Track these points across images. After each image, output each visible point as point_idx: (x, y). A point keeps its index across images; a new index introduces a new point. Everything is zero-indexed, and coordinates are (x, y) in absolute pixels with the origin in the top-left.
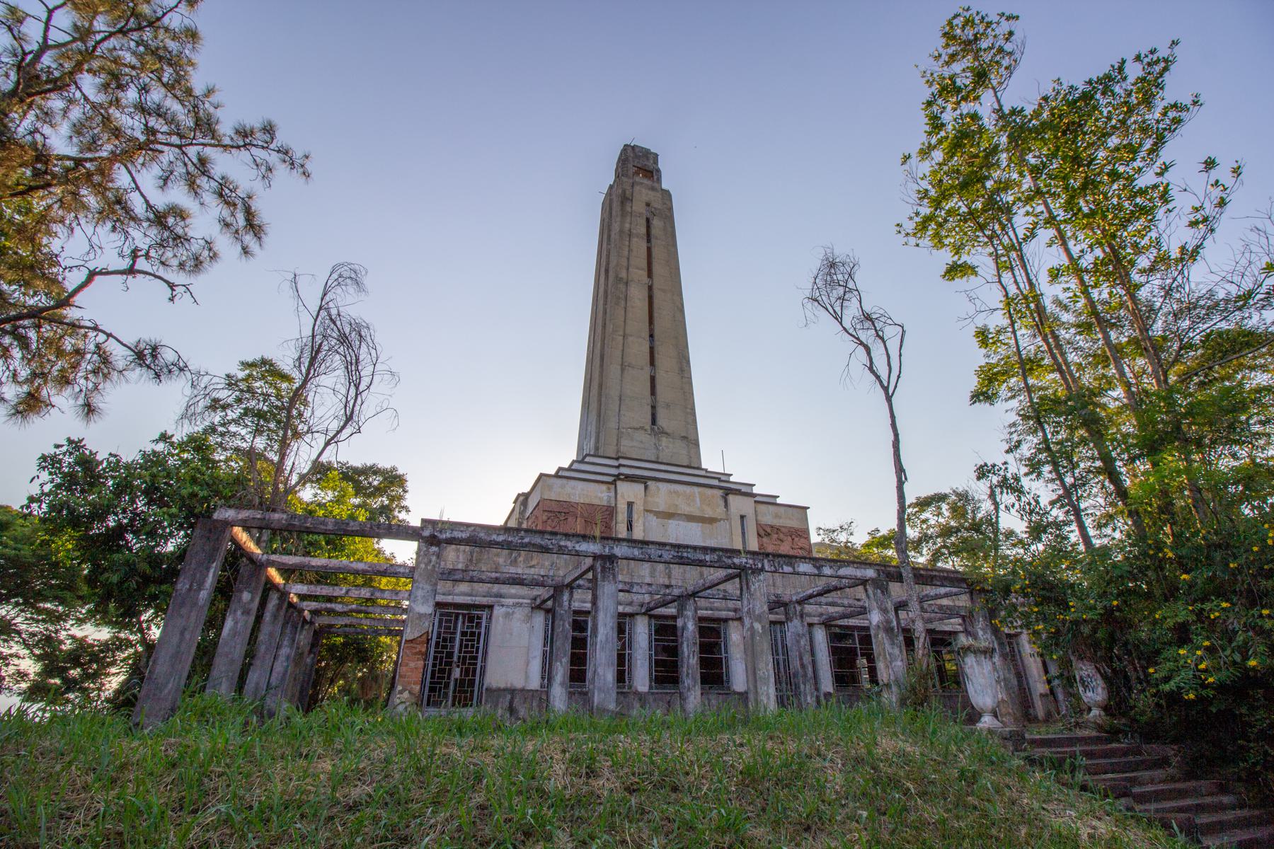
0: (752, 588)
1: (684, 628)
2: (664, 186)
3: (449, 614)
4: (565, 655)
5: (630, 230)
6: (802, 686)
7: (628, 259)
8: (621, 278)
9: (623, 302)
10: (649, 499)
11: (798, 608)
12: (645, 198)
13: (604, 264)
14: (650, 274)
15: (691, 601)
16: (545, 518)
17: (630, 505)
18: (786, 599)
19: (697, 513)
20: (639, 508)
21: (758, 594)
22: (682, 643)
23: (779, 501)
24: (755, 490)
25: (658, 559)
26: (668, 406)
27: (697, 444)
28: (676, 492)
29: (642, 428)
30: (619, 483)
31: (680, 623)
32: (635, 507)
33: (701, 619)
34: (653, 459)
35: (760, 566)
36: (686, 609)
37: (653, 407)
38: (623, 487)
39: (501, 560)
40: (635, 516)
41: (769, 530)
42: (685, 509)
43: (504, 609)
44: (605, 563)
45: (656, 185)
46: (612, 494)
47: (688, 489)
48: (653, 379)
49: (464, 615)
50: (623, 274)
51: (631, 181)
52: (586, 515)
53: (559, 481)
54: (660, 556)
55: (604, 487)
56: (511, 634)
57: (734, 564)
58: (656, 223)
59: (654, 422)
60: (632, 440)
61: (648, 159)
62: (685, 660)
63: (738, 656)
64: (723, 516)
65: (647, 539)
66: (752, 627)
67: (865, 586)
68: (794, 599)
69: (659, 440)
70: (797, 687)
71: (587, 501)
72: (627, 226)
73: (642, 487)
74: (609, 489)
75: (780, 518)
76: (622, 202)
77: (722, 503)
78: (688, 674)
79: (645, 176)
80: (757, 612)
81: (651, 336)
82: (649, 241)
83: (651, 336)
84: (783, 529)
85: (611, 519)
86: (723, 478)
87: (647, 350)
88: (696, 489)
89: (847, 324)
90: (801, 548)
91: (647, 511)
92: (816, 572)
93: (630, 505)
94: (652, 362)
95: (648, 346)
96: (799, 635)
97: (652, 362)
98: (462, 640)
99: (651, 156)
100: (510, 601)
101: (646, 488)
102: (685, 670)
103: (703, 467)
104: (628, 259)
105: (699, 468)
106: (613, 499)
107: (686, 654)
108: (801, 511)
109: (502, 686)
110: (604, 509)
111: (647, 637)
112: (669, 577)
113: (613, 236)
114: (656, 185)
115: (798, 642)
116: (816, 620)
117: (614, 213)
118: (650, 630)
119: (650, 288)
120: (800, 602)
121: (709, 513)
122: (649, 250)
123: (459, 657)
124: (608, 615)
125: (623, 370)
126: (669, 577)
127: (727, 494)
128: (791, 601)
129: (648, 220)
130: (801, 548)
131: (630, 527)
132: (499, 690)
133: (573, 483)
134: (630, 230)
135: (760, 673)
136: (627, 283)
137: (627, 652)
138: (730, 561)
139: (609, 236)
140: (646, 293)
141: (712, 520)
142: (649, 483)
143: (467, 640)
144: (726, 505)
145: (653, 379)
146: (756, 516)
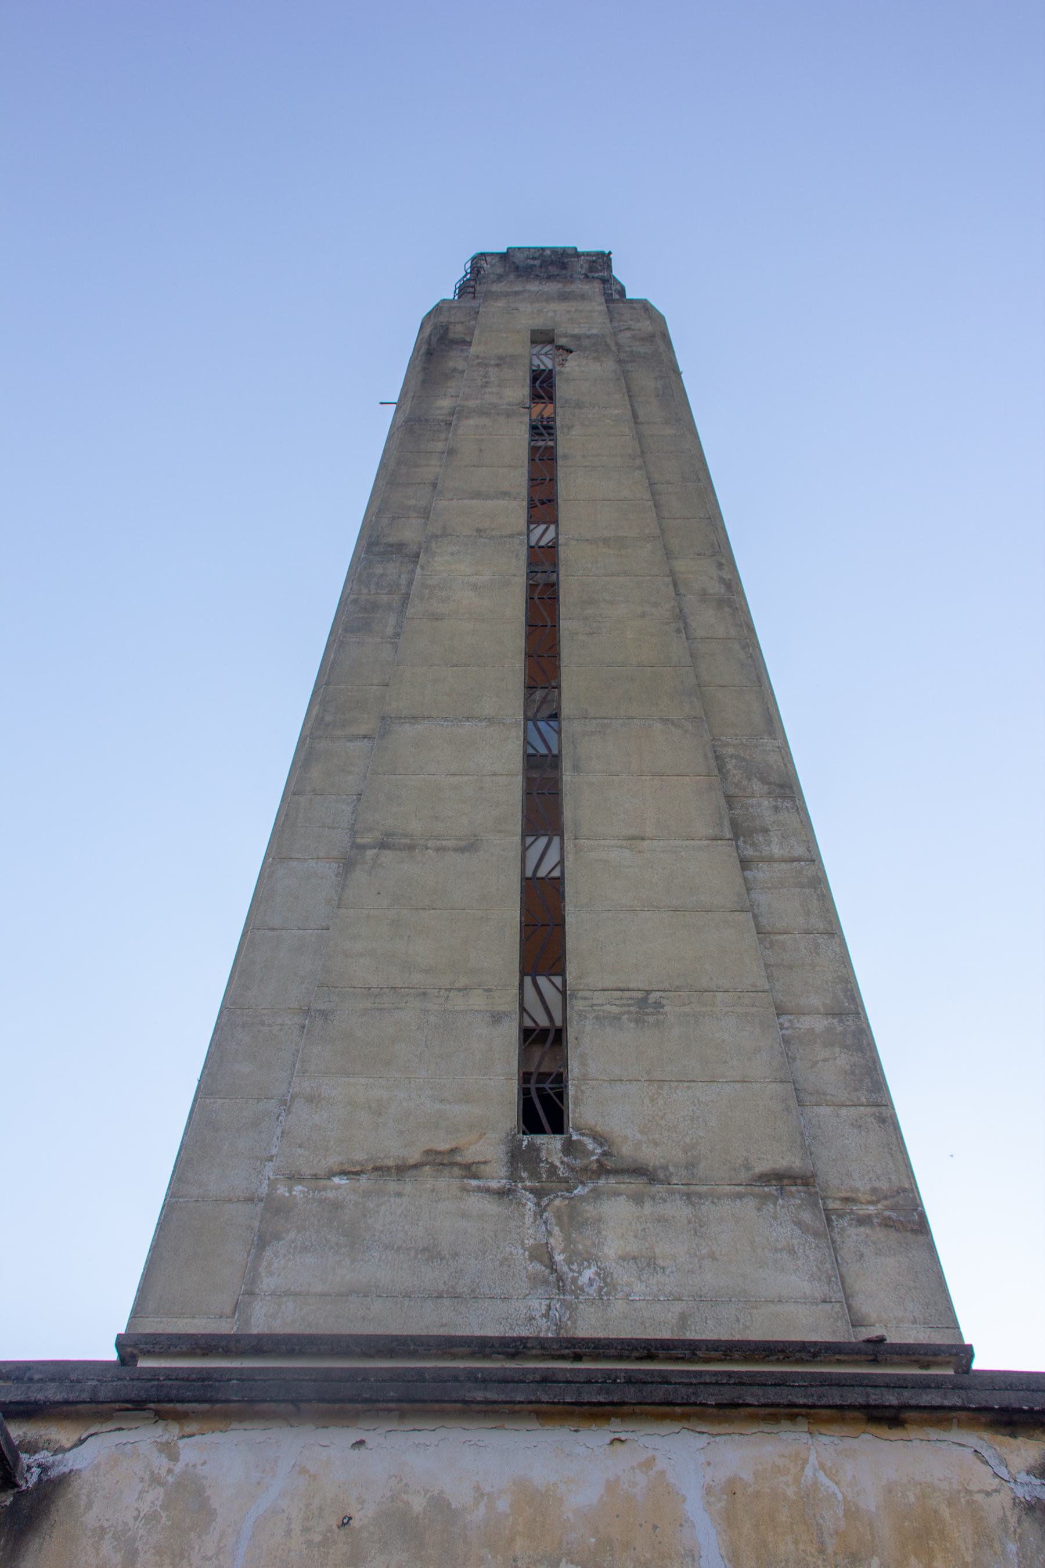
9: (392, 619)
27: (920, 1227)
125: (348, 864)
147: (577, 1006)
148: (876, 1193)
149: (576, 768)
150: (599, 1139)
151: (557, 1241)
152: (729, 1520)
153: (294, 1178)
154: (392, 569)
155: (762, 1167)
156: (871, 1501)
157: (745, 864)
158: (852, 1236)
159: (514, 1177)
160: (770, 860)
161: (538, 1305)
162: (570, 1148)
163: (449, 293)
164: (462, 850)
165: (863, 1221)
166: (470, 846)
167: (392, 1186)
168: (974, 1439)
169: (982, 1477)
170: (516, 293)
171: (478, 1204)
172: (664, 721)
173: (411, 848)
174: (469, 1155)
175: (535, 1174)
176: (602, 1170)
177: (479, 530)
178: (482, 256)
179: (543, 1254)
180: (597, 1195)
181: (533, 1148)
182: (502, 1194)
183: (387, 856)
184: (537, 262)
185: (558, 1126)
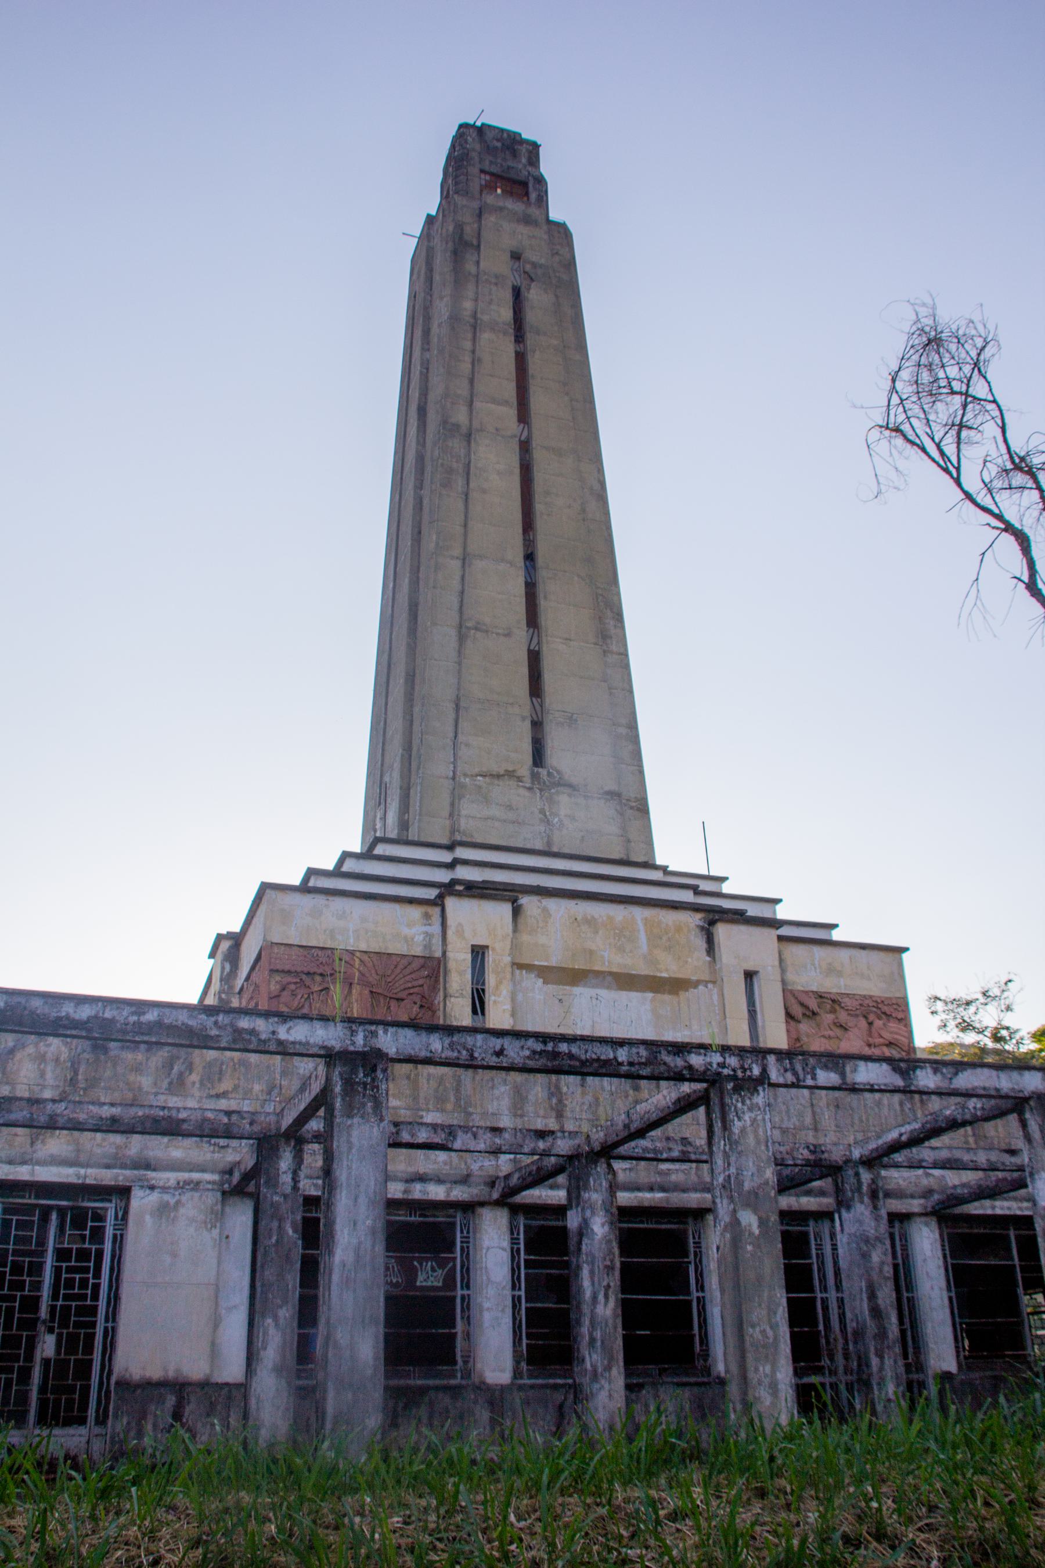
0: (737, 1126)
1: (584, 1230)
2: (554, 215)
3: (29, 1209)
4: (285, 1301)
5: (474, 315)
6: (875, 1361)
7: (472, 381)
8: (457, 426)
9: (460, 482)
10: (525, 938)
11: (866, 1176)
12: (508, 242)
13: (415, 395)
14: (524, 415)
15: (601, 1168)
16: (274, 987)
17: (479, 953)
18: (836, 1155)
19: (642, 969)
20: (498, 960)
21: (751, 1140)
22: (579, 1267)
23: (836, 935)
24: (782, 913)
25: (493, 1061)
27: (643, 809)
28: (590, 922)
29: (510, 774)
30: (450, 902)
31: (573, 1221)
32: (490, 958)
33: (625, 1213)
34: (539, 845)
35: (756, 1071)
36: (586, 1187)
37: (537, 725)
38: (457, 909)
39: (146, 1082)
40: (491, 980)
41: (813, 1004)
42: (612, 960)
43: (154, 1197)
44: (354, 1071)
45: (534, 212)
46: (436, 929)
47: (618, 913)
48: (534, 659)
49: (62, 1211)
50: (460, 416)
51: (476, 205)
52: (373, 978)
53: (308, 901)
54: (499, 1053)
55: (415, 913)
56: (174, 1255)
57: (690, 1067)
58: (536, 297)
59: (538, 756)
60: (487, 801)
61: (515, 154)
62: (586, 1309)
64: (706, 977)
65: (519, 1027)
66: (735, 1222)
67: (1021, 1114)
68: (856, 1154)
69: (551, 801)
70: (863, 1362)
71: (375, 947)
72: (468, 305)
73: (506, 909)
74: (427, 916)
75: (840, 974)
76: (455, 253)
77: (701, 943)
78: (592, 1341)
79: (508, 193)
80: (747, 1186)
81: (530, 557)
82: (519, 337)
83: (530, 557)
84: (847, 1002)
85: (434, 988)
86: (704, 886)
87: (520, 589)
88: (639, 913)
89: (971, 482)
90: (890, 1044)
91: (521, 966)
92: (900, 1082)
93: (479, 953)
95: (521, 581)
96: (867, 1241)
98: (57, 1271)
99: (523, 149)
100: (171, 1178)
101: (517, 912)
102: (585, 1330)
103: (659, 861)
104: (472, 381)
105: (649, 865)
106: (437, 941)
107: (588, 1294)
108: (888, 957)
109: (155, 1373)
110: (415, 965)
111: (505, 1256)
112: (560, 1115)
113: (435, 329)
114: (534, 212)
115: (865, 1256)
116: (915, 1205)
117: (437, 278)
118: (514, 1241)
119: (525, 447)
120: (872, 1162)
121: (668, 967)
122: (521, 359)
123: (52, 1309)
124: (363, 1200)
126: (560, 1115)
127: (712, 923)
128: (847, 1161)
129: (517, 294)
130: (890, 1044)
131: (479, 1003)
132: (148, 1385)
133: (339, 904)
134: (474, 315)
135: (754, 1334)
136: (468, 437)
137: (459, 1292)
138: (679, 1062)
139: (426, 333)
140: (514, 461)
141: (676, 986)
142: (524, 900)
143: (69, 1270)
144: (710, 940)
145: (534, 659)
146: (783, 970)
149: (545, 598)
150: (558, 772)
151: (547, 808)
152: (645, 925)
155: (607, 788)
156: (670, 923)
159: (533, 783)
160: (612, 652)
161: (543, 829)
162: (549, 774)
166: (508, 635)
167: (496, 782)
168: (690, 913)
169: (690, 920)
170: (501, 209)
171: (522, 791)
172: (579, 576)
174: (519, 773)
175: (539, 783)
176: (559, 784)
177: (497, 430)
179: (542, 812)
180: (558, 793)
182: (530, 789)
183: (479, 634)
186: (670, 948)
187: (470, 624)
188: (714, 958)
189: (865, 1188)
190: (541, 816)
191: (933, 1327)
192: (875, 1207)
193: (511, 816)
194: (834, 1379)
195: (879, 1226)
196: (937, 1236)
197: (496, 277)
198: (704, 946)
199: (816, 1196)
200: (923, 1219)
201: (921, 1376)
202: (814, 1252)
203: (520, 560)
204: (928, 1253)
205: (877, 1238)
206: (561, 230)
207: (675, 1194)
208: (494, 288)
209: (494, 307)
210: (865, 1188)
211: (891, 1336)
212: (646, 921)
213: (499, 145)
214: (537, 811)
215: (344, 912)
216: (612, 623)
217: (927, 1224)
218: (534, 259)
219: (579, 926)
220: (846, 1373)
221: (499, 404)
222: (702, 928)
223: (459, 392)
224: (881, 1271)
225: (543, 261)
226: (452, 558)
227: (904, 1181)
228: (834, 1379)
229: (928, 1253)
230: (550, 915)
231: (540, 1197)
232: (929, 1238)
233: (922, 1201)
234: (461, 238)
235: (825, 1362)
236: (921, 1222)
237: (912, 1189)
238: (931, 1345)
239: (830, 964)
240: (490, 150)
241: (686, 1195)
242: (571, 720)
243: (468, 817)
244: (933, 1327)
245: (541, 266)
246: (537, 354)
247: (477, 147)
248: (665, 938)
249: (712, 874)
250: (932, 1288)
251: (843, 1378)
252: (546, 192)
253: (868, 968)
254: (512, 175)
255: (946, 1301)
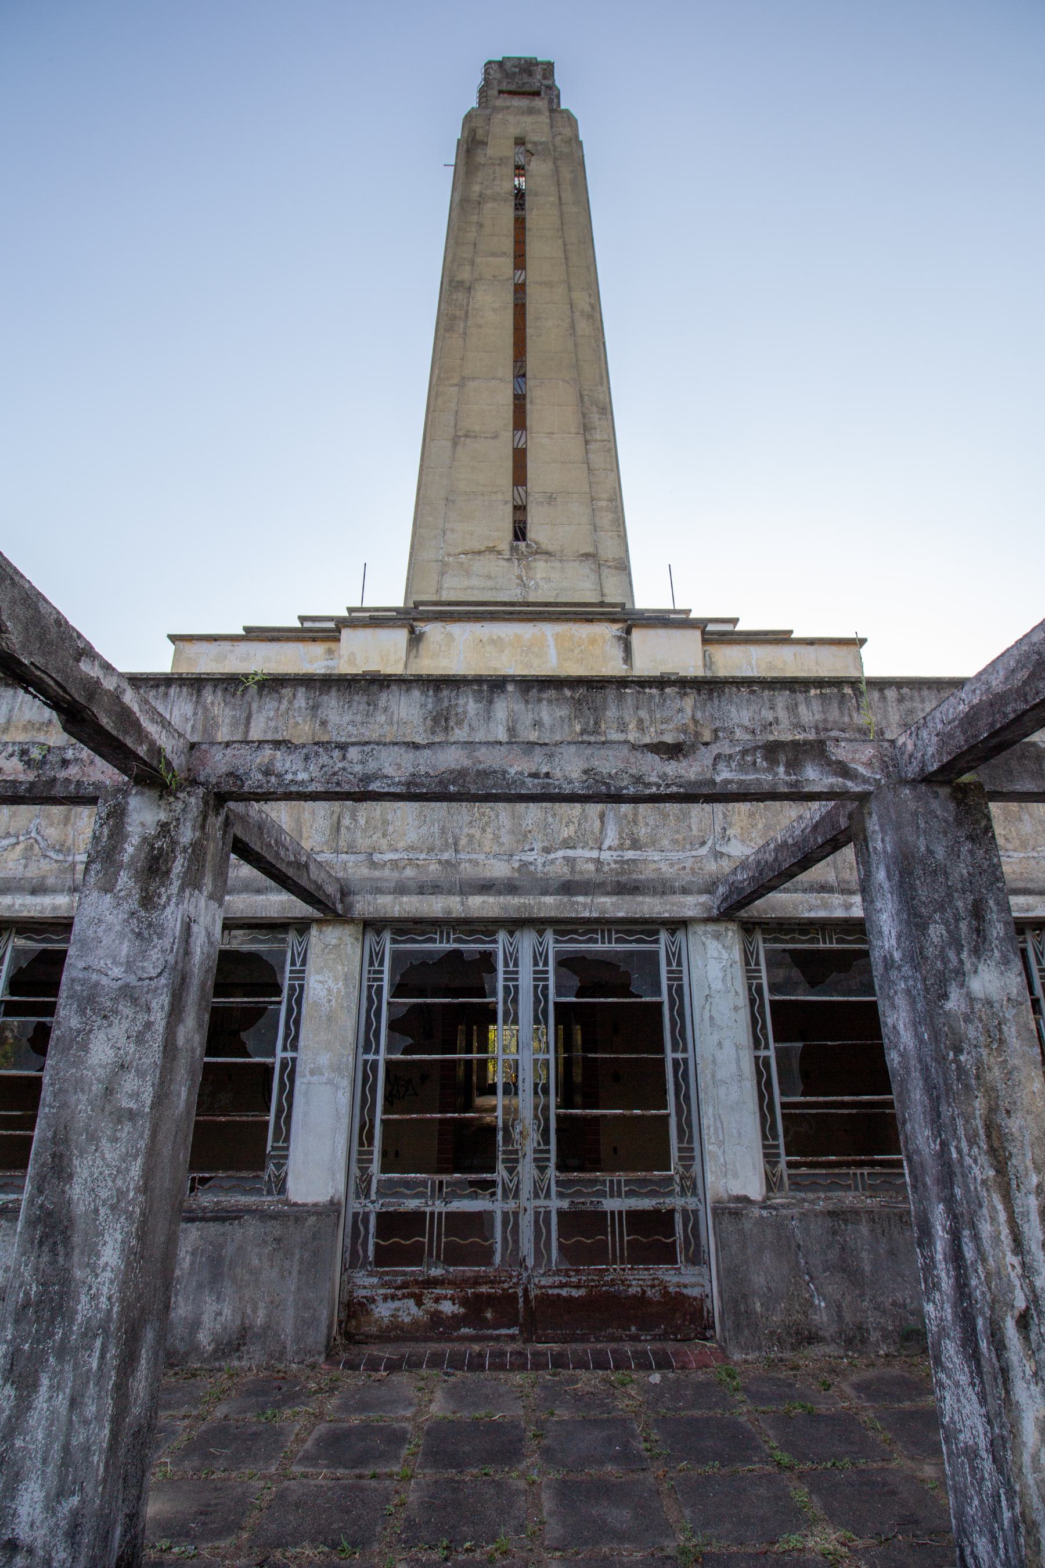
2: (563, 107)
8: (462, 282)
9: (462, 325)
12: (513, 131)
14: (520, 260)
26: (551, 499)
29: (491, 550)
48: (520, 457)
59: (520, 533)
60: (468, 574)
61: (530, 74)
63: (324, 1059)
69: (528, 568)
72: (477, 188)
94: (520, 421)
95: (510, 393)
97: (520, 421)
99: (539, 70)
108: (844, 650)
116: (690, 906)
119: (520, 289)
122: (520, 224)
125: (455, 444)
127: (628, 632)
140: (509, 298)
145: (520, 457)
147: (530, 498)
148: (614, 559)
149: (531, 402)
150: (536, 543)
151: (524, 574)
152: (556, 640)
153: (449, 555)
154: (460, 296)
155: (582, 552)
156: (584, 636)
157: (587, 442)
158: (605, 572)
159: (512, 555)
160: (596, 441)
161: (519, 592)
162: (528, 546)
163: (474, 103)
164: (492, 438)
165: (609, 567)
166: (495, 437)
167: (477, 558)
168: (606, 624)
169: (607, 631)
170: (508, 108)
172: (563, 380)
173: (476, 437)
174: (498, 548)
175: (518, 554)
176: (537, 553)
178: (490, 63)
179: (520, 577)
180: (535, 560)
181: (517, 546)
182: (508, 560)
183: (468, 441)
184: (517, 70)
185: (524, 540)
186: (582, 660)
187: (460, 434)
188: (631, 666)
189: (130, 848)
190: (518, 581)
191: (717, 1117)
192: (148, 901)
193: (490, 583)
194: (511, 1205)
195: (143, 954)
196: (737, 954)
197: (501, 159)
198: (622, 654)
199: (499, 893)
200: (711, 927)
201: (691, 1203)
202: (500, 984)
203: (509, 376)
204: (717, 985)
205: (128, 993)
206: (565, 115)
207: (244, 896)
208: (497, 168)
209: (497, 182)
210: (130, 848)
211: (83, 1307)
212: (557, 636)
213: (517, 70)
214: (514, 577)
215: (248, 654)
216: (597, 416)
217: (717, 937)
218: (536, 139)
219: (483, 647)
220: (537, 1196)
221: (498, 256)
222: (620, 638)
223: (465, 255)
224: (109, 1092)
225: (544, 139)
226: (452, 385)
227: (672, 865)
228: (511, 1205)
229: (717, 985)
230: (453, 639)
231: (10, 907)
232: (719, 959)
233: (704, 898)
234: (473, 139)
235: (501, 1173)
236: (705, 933)
237: (687, 878)
238: (710, 1147)
239: (770, 662)
240: (508, 76)
241: (262, 897)
242: (551, 499)
243: (449, 589)
244: (717, 1117)
245: (541, 143)
246: (535, 212)
247: (499, 76)
248: (576, 651)
249: (678, 607)
250: (720, 1045)
251: (531, 1205)
252: (558, 97)
253: (817, 664)
254: (527, 88)
255: (748, 1068)
